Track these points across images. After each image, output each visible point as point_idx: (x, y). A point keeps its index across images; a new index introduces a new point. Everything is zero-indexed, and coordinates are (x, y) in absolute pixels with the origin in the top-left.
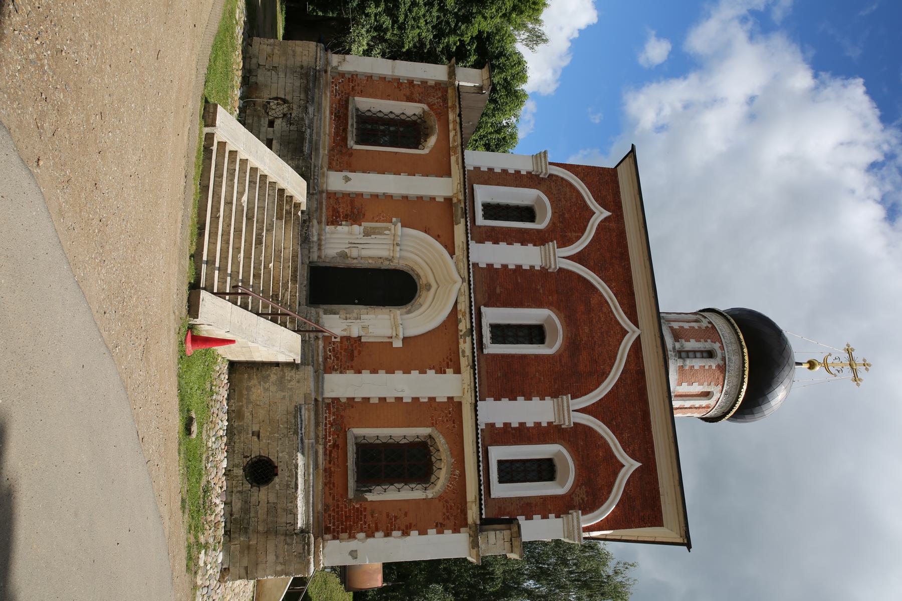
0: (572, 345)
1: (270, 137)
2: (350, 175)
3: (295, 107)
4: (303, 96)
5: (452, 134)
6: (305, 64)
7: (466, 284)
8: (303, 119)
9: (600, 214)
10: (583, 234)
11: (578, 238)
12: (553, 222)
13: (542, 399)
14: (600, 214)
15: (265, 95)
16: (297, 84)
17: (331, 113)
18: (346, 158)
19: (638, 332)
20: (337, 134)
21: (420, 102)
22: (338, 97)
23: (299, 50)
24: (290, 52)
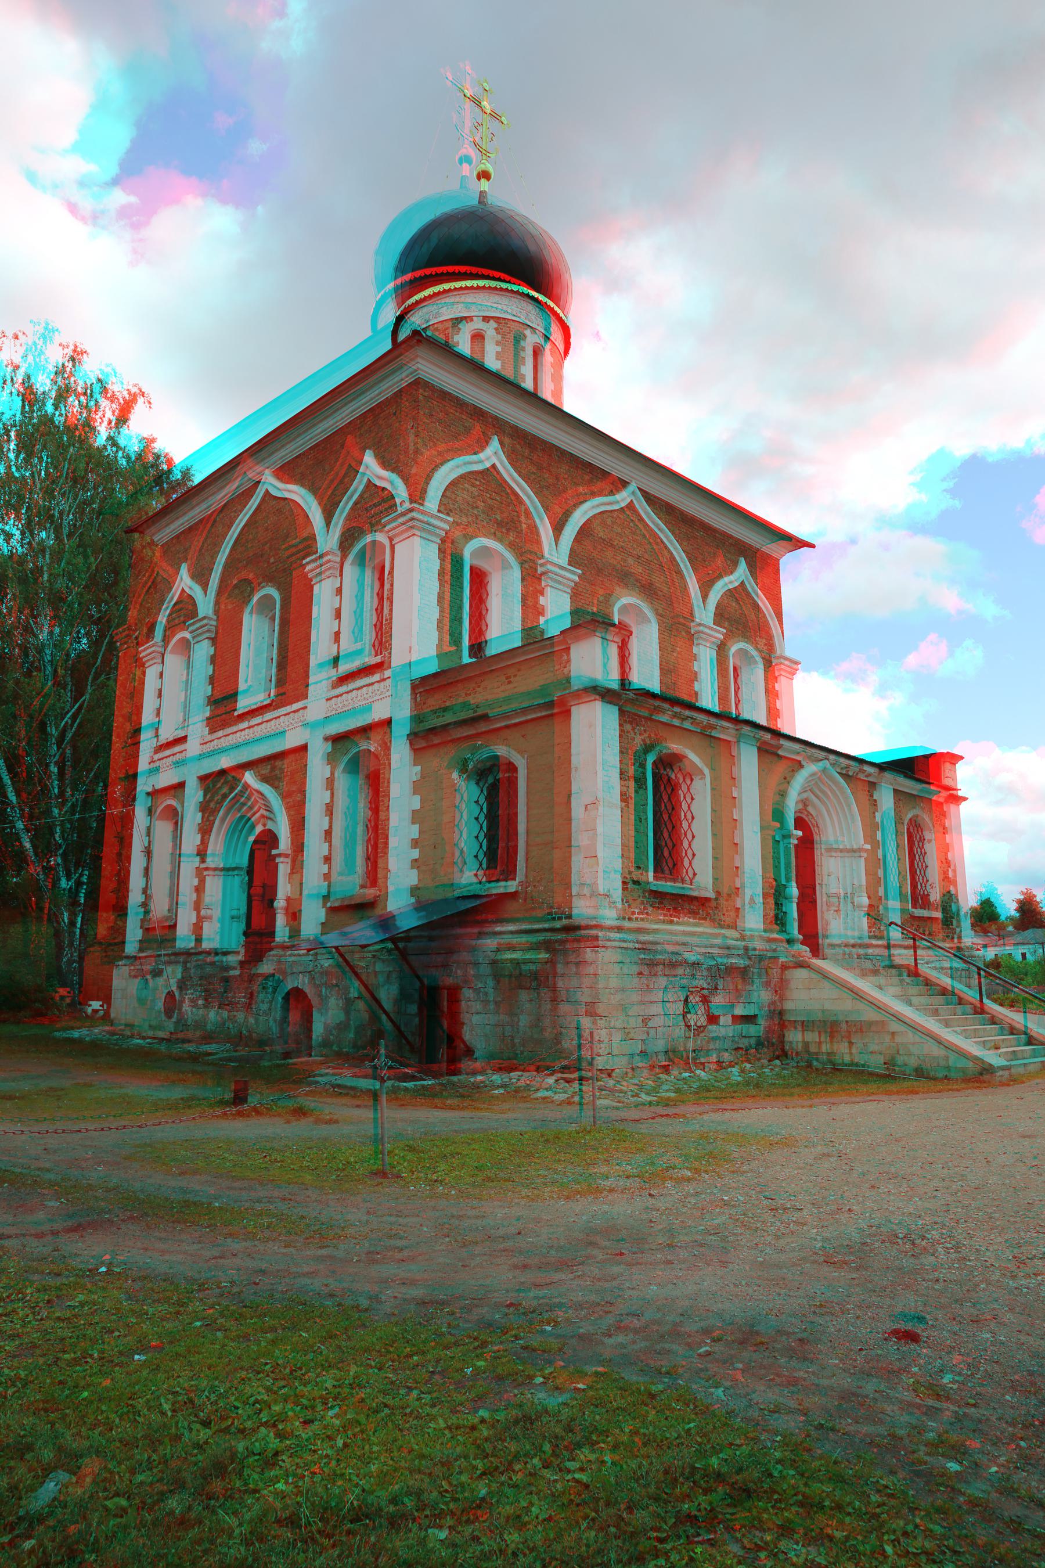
0: (648, 591)
1: (730, 1019)
2: (748, 893)
3: (695, 983)
4: (680, 971)
5: (687, 725)
6: (635, 969)
7: (832, 757)
8: (709, 969)
9: (492, 455)
10: (521, 502)
11: (528, 513)
12: (511, 546)
13: (694, 657)
14: (492, 455)
15: (679, 1032)
16: (662, 981)
17: (672, 922)
18: (722, 901)
19: (633, 487)
20: (694, 914)
21: (643, 766)
22: (650, 910)
23: (614, 982)
24: (618, 997)
